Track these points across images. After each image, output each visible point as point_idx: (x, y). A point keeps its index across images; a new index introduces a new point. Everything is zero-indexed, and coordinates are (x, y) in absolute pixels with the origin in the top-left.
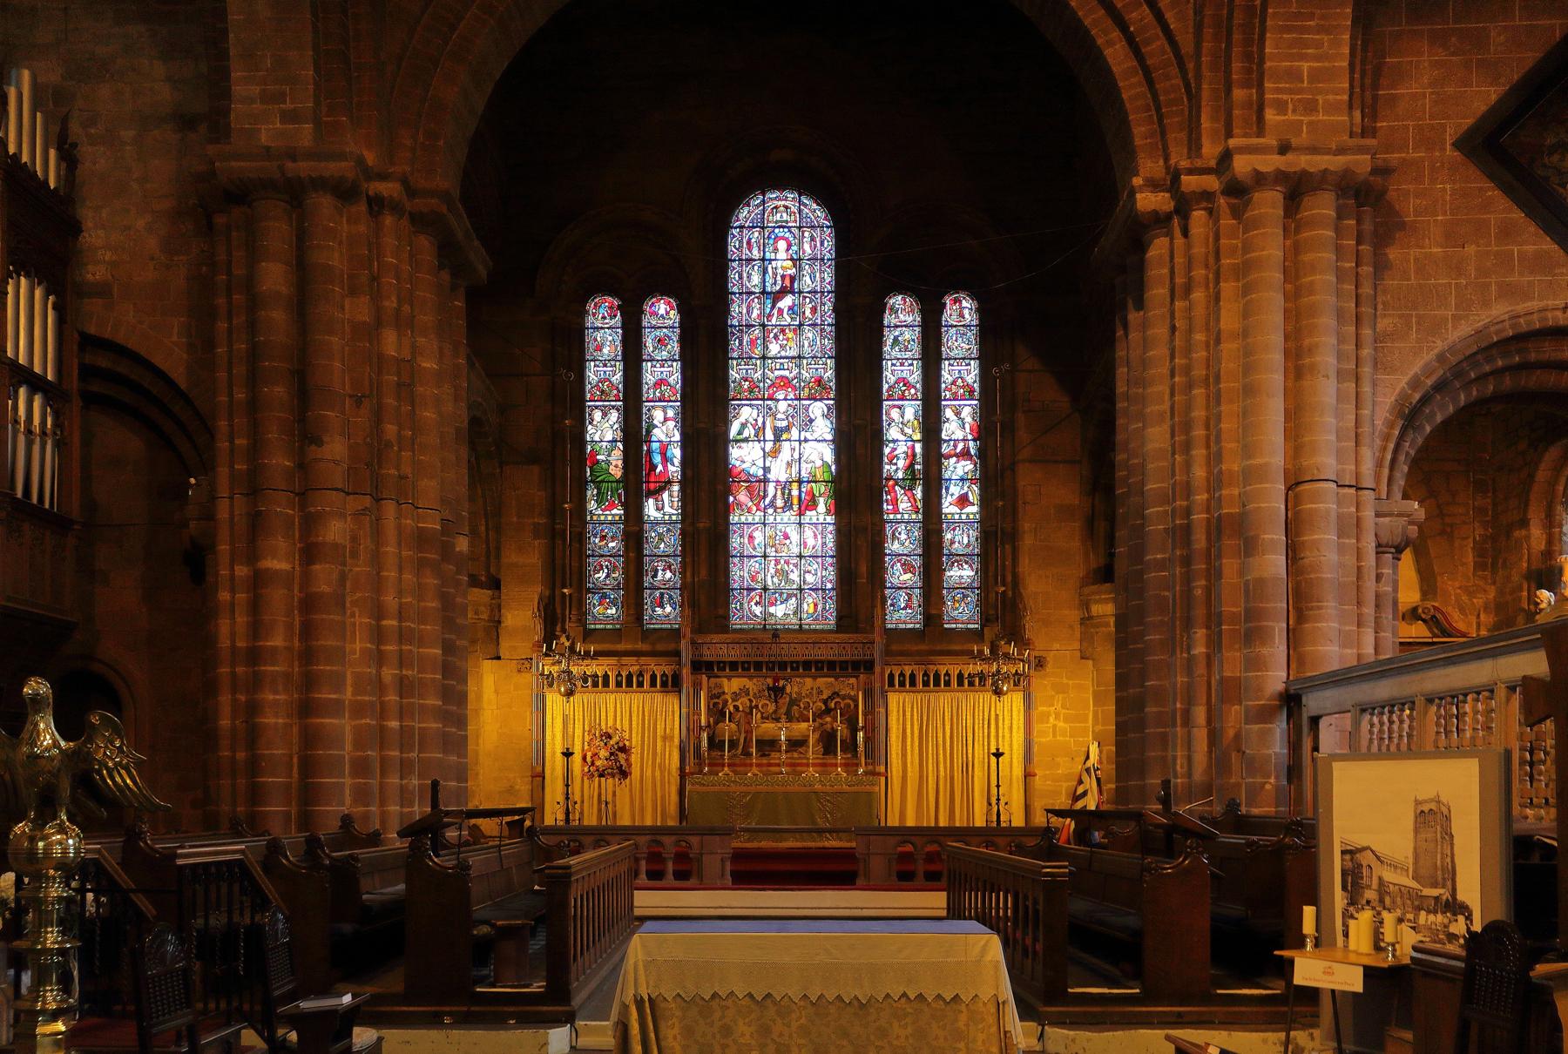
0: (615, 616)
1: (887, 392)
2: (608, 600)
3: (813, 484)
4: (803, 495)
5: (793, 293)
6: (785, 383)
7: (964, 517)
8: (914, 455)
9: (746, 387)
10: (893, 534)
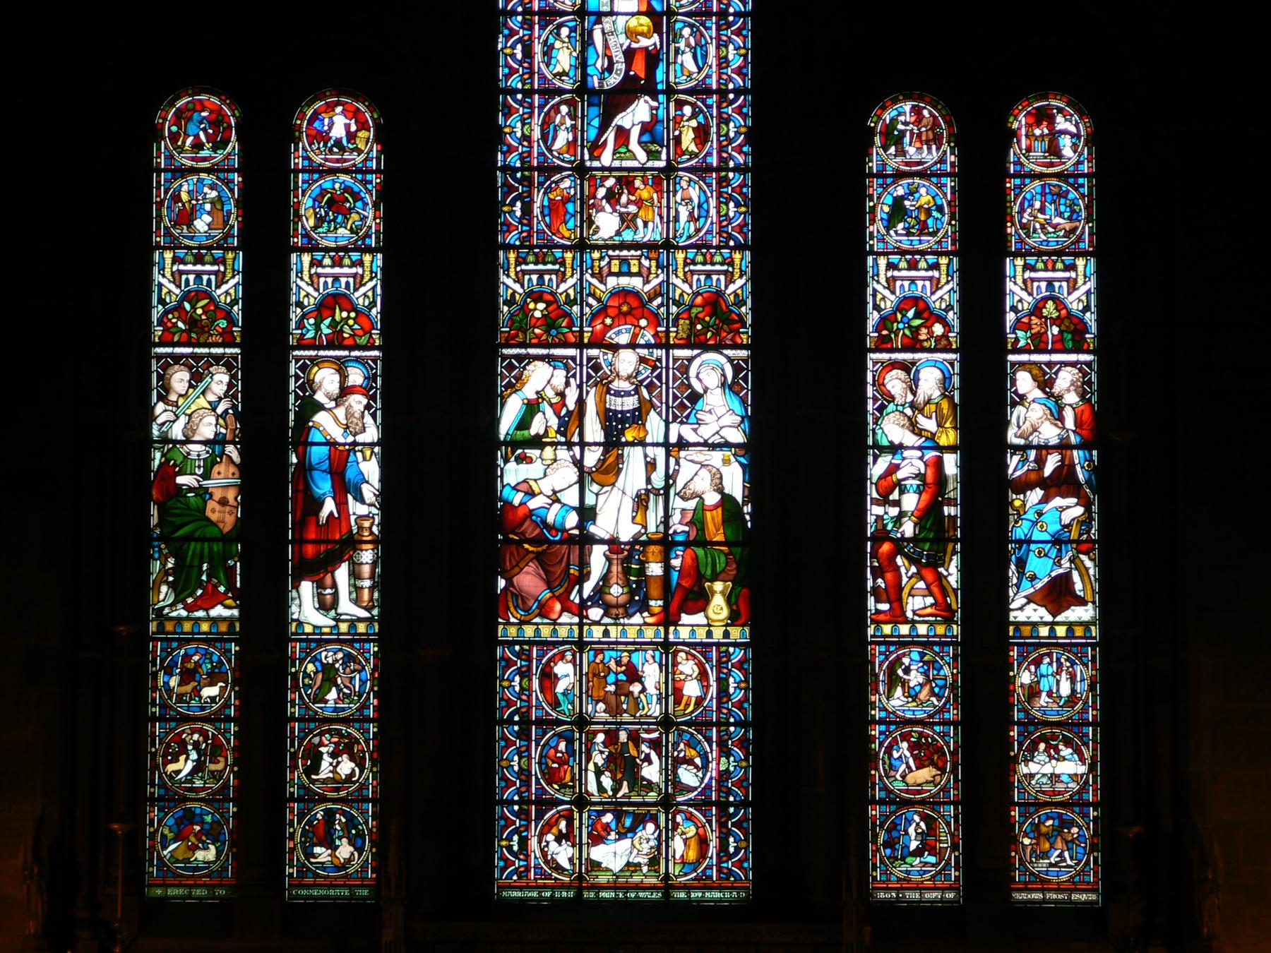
1: (878, 329)
3: (700, 552)
4: (675, 575)
8: (941, 479)
9: (538, 314)
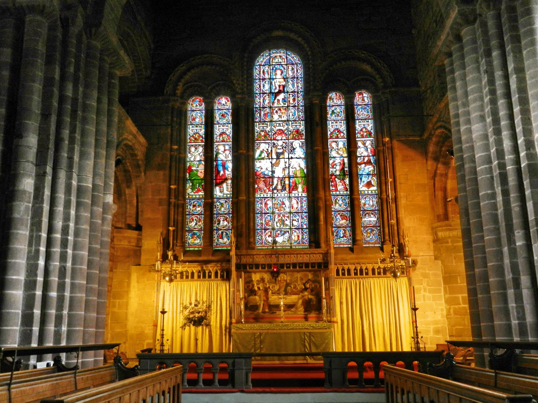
0: (199, 244)
1: (330, 135)
2: (196, 236)
3: (296, 179)
4: (291, 184)
5: (284, 92)
6: (281, 132)
7: (370, 192)
8: (344, 164)
9: (263, 135)
10: (336, 201)
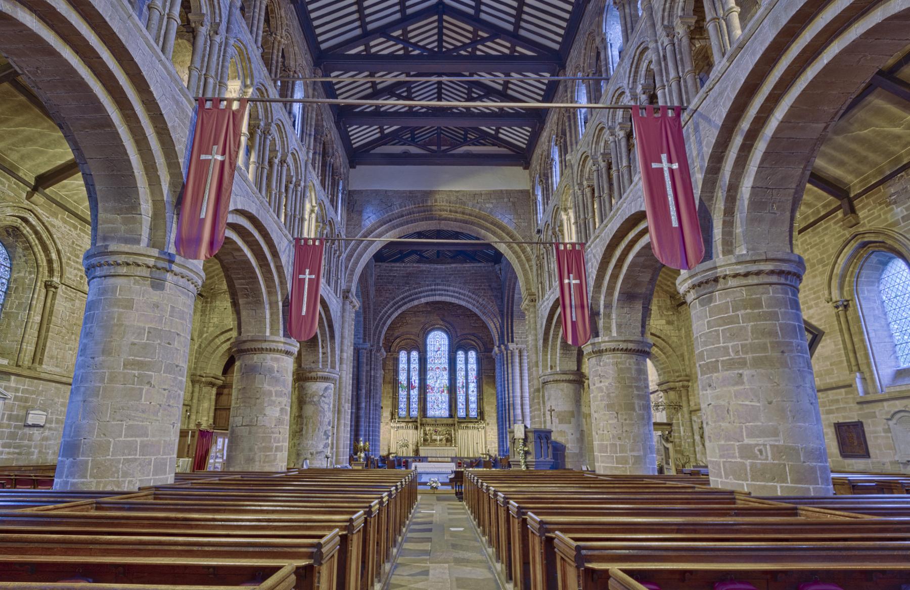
6: (438, 368)
